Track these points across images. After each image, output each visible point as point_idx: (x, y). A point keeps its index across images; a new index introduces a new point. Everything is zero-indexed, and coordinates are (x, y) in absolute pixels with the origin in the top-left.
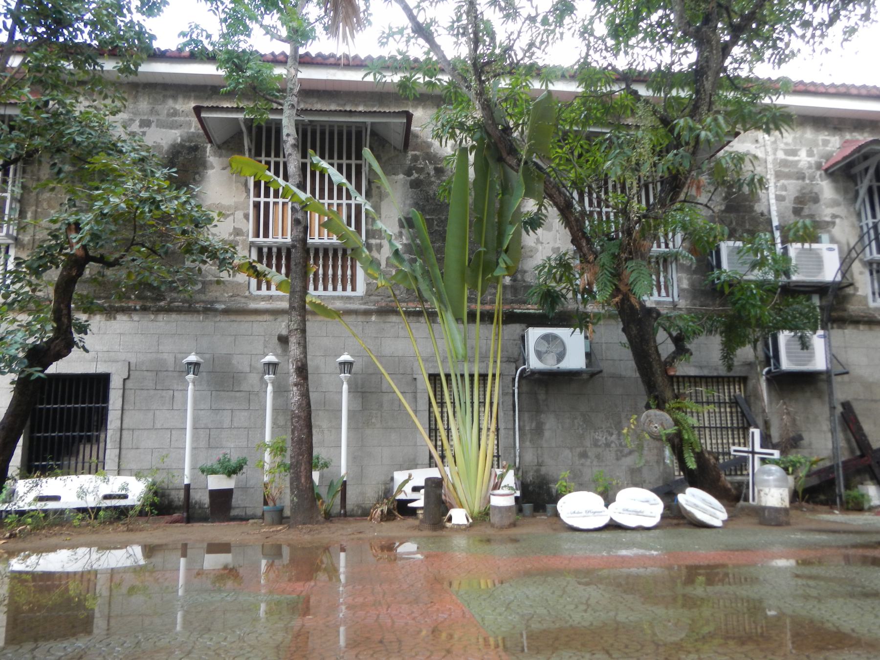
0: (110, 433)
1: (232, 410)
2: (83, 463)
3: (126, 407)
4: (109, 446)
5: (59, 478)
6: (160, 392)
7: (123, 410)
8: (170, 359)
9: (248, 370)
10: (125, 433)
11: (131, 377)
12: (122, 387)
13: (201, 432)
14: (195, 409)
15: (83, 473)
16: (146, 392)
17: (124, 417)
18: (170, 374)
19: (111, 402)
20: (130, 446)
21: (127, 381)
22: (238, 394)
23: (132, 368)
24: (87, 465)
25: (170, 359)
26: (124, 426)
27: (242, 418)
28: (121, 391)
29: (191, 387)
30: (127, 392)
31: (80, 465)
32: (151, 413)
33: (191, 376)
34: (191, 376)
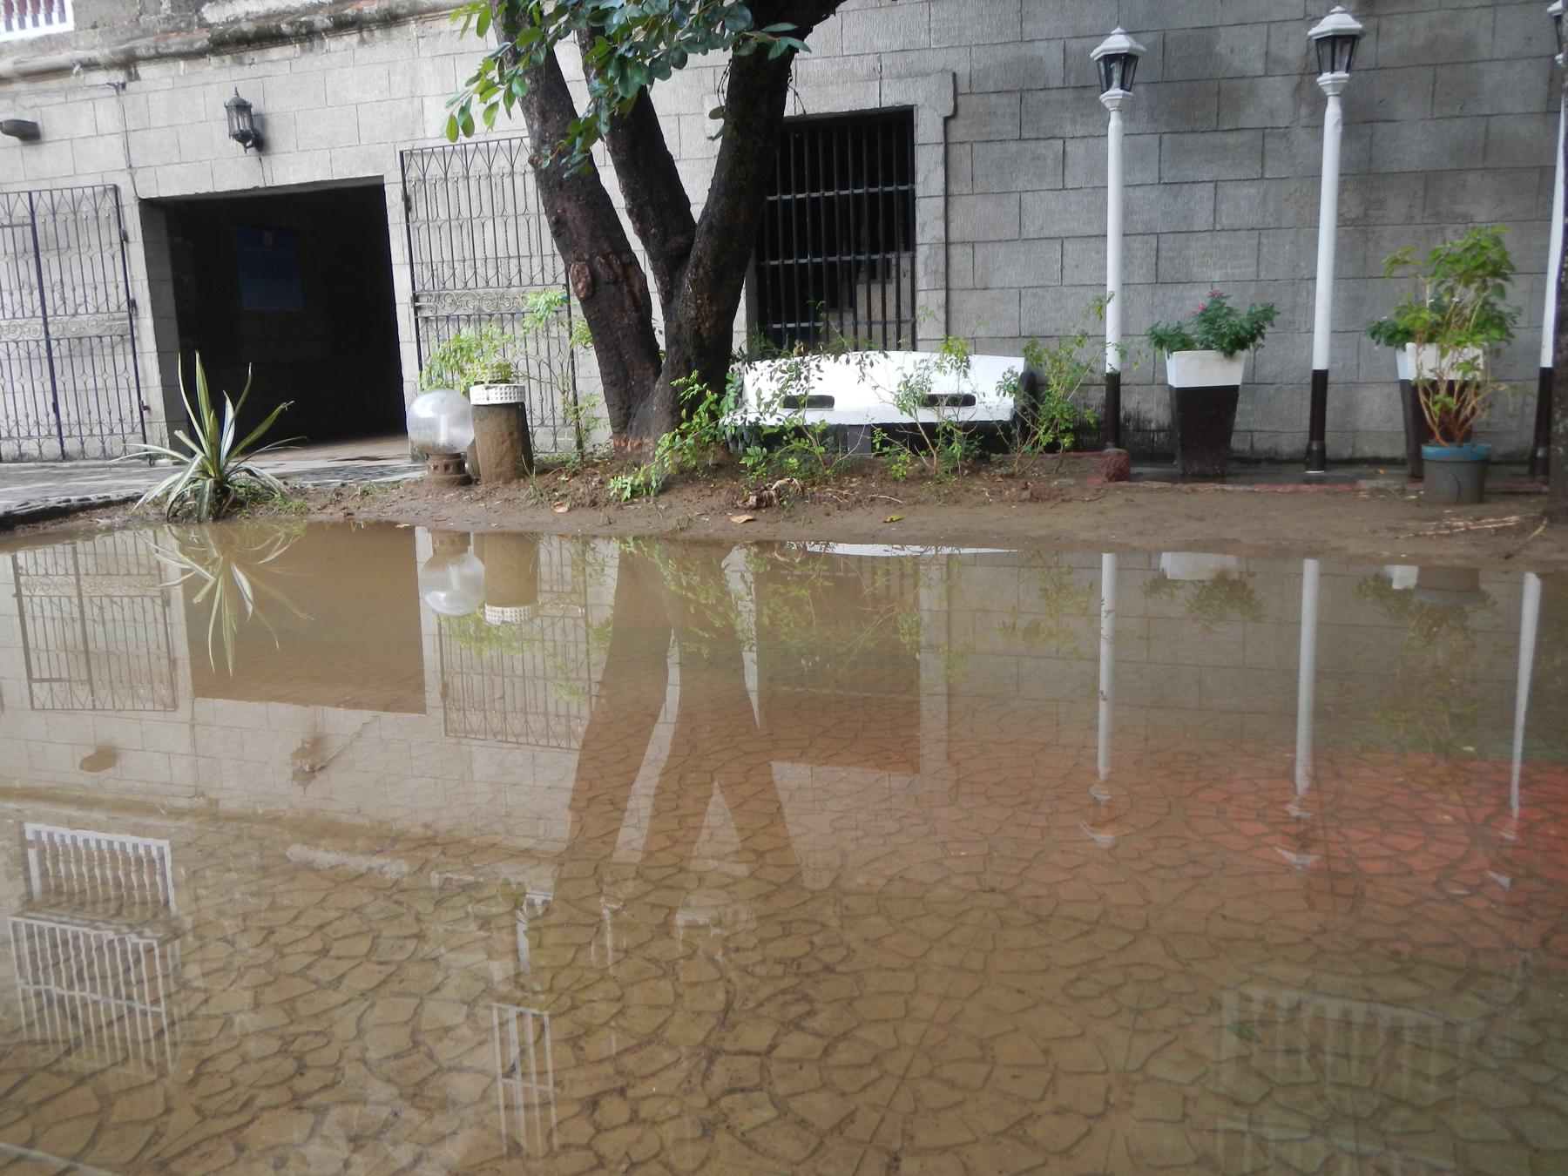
0: (922, 253)
1: (1216, 182)
2: (870, 323)
3: (954, 188)
4: (922, 283)
5: (843, 357)
6: (1031, 145)
7: (947, 195)
8: (1051, 55)
9: (1258, 67)
10: (955, 251)
11: (961, 112)
12: (941, 139)
13: (1136, 243)
14: (1127, 186)
15: (898, 347)
16: (996, 147)
17: (951, 212)
18: (1054, 95)
19: (919, 178)
20: (970, 284)
21: (952, 123)
22: (1232, 139)
23: (963, 88)
24: (877, 329)
25: (1051, 55)
26: (954, 237)
27: (1242, 202)
28: (941, 149)
29: (1114, 123)
30: (956, 151)
31: (863, 329)
32: (1015, 197)
33: (1115, 92)
34: (1115, 92)
